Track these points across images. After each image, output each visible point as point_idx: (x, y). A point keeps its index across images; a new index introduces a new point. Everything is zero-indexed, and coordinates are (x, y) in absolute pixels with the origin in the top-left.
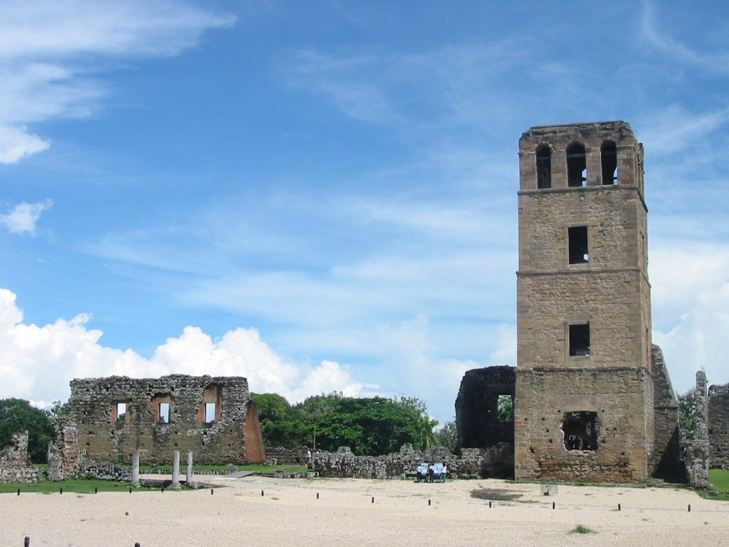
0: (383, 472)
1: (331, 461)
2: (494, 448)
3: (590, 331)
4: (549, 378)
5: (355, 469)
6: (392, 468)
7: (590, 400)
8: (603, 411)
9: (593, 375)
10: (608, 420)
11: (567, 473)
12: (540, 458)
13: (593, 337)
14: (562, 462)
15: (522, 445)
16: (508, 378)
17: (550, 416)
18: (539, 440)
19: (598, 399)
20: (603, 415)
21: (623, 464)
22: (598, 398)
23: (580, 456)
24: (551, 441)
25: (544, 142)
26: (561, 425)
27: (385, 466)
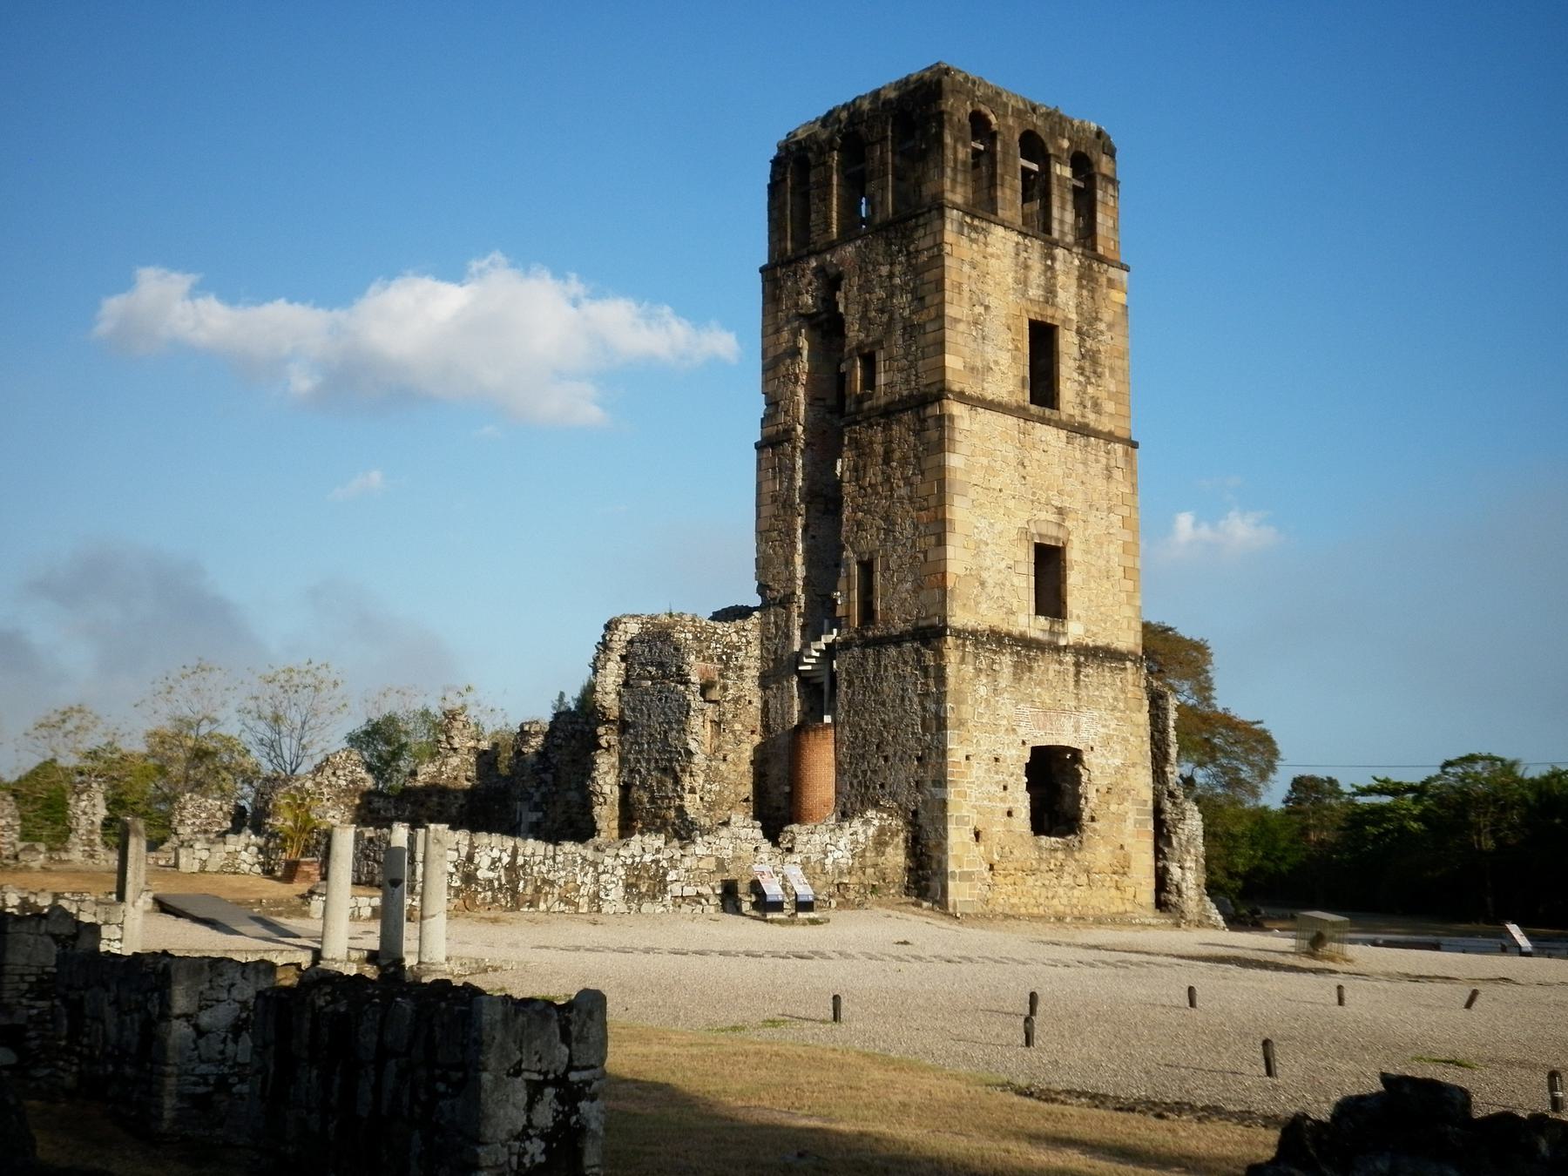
0: (617, 892)
1: (476, 861)
2: (857, 824)
4: (1006, 660)
5: (545, 881)
6: (638, 877)
8: (1092, 749)
9: (1077, 665)
10: (1098, 771)
11: (1036, 892)
14: (1029, 864)
15: (961, 821)
16: (708, 648)
17: (1008, 754)
18: (992, 811)
20: (1092, 755)
24: (1010, 814)
27: (621, 872)
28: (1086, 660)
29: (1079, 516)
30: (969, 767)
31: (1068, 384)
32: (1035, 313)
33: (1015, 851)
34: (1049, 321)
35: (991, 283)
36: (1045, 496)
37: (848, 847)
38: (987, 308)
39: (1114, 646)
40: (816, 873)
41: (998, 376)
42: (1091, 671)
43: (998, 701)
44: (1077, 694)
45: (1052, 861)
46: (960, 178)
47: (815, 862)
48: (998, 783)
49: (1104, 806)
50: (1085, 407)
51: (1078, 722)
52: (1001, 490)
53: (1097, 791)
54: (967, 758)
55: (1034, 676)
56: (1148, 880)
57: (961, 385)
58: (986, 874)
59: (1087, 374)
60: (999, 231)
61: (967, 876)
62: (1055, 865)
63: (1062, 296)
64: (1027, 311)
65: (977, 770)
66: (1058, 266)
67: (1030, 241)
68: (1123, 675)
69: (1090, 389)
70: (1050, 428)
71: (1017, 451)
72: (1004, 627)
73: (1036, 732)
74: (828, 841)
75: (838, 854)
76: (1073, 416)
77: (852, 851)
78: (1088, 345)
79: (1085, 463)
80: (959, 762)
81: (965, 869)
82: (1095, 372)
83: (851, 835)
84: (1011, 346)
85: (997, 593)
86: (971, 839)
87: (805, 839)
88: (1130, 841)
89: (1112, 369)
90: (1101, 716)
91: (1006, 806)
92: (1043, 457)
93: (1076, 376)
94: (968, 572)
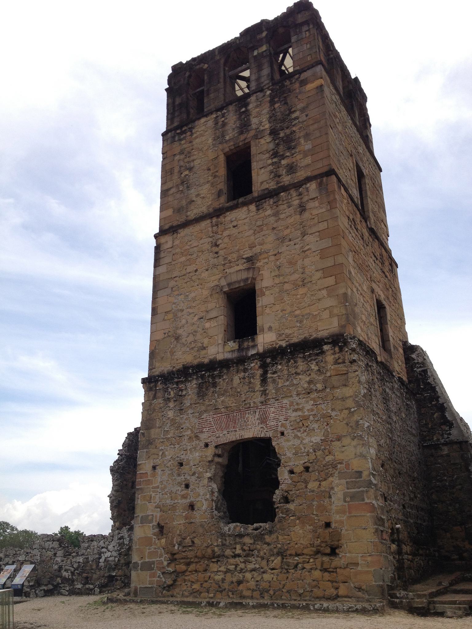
3: (258, 292)
4: (192, 387)
7: (257, 416)
8: (282, 434)
9: (264, 367)
11: (218, 577)
12: (174, 546)
13: (261, 302)
14: (209, 551)
15: (145, 520)
18: (173, 508)
19: (272, 411)
20: (282, 439)
21: (328, 551)
22: (272, 409)
23: (241, 536)
25: (198, 67)
26: (209, 475)
28: (274, 358)
29: (270, 254)
30: (154, 475)
31: (263, 170)
32: (229, 147)
33: (196, 541)
34: (240, 144)
35: (195, 153)
36: (235, 256)
37: (116, 548)
38: (190, 169)
39: (314, 336)
40: (92, 569)
41: (199, 201)
42: (280, 367)
43: (182, 418)
44: (266, 390)
45: (238, 547)
46: (177, 114)
47: (93, 561)
48: (180, 484)
49: (301, 485)
50: (279, 176)
51: (265, 413)
52: (196, 271)
53: (291, 472)
54: (154, 468)
55: (217, 389)
56: (369, 559)
57: (171, 224)
58: (165, 563)
59: (281, 153)
60: (203, 120)
61: (147, 566)
62: (244, 550)
63: (254, 121)
64: (222, 150)
65: (160, 477)
66: (251, 106)
67: (226, 110)
68: (320, 358)
69: (284, 162)
70: (240, 209)
71: (211, 239)
72: (196, 362)
73: (218, 433)
74: (103, 545)
75: (109, 554)
76: (267, 188)
77: (120, 551)
78: (282, 135)
79: (276, 214)
80: (147, 473)
81: (147, 560)
82: (289, 148)
83: (120, 539)
84: (210, 178)
85: (191, 338)
86: (154, 534)
87: (86, 545)
88: (337, 517)
89: (307, 136)
90: (291, 404)
91: (188, 501)
92: (235, 231)
93: (270, 161)
94: (166, 334)
